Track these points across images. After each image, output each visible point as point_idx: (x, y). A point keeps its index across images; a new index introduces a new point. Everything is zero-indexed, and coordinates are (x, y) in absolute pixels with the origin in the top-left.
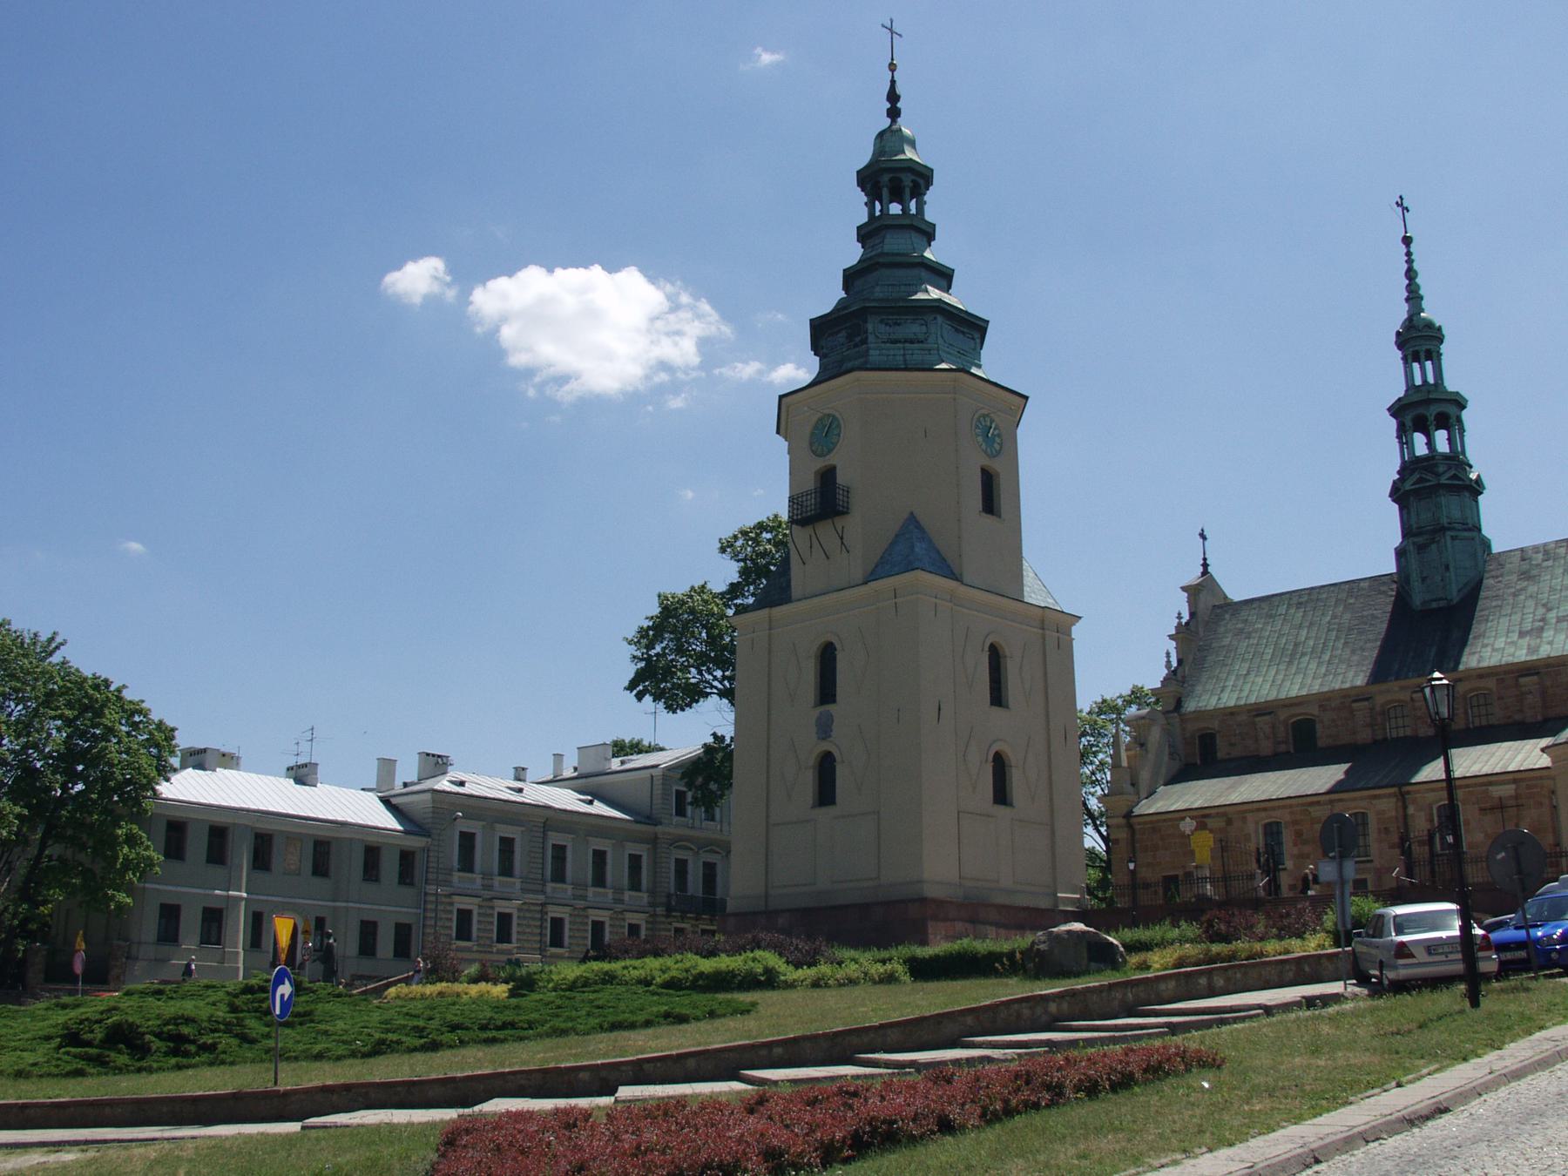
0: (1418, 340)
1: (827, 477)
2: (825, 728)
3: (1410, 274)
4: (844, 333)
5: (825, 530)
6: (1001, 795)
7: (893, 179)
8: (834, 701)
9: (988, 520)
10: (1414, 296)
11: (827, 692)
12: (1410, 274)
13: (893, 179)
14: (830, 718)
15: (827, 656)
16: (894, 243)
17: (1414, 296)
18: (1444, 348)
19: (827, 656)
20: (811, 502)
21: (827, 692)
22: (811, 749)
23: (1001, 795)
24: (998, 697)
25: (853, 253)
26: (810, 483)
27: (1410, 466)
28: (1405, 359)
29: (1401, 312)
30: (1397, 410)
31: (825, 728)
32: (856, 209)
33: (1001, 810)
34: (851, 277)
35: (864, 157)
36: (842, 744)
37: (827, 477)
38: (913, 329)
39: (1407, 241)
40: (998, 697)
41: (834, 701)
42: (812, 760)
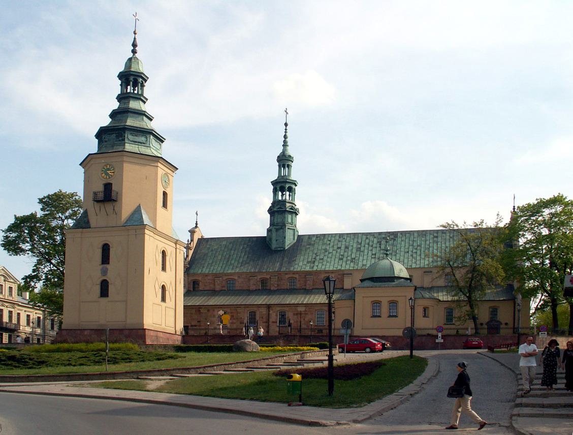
0: (284, 160)
1: (108, 187)
2: (104, 272)
3: (285, 137)
4: (115, 135)
5: (109, 206)
6: (163, 299)
7: (131, 79)
8: (108, 263)
9: (163, 210)
10: (285, 144)
11: (105, 259)
12: (285, 137)
13: (131, 79)
14: (107, 269)
15: (106, 249)
16: (133, 104)
17: (285, 144)
18: (293, 164)
19: (106, 249)
20: (101, 196)
21: (105, 259)
22: (98, 278)
23: (163, 299)
24: (164, 269)
25: (116, 105)
26: (101, 188)
27: (276, 203)
28: (279, 166)
29: (280, 150)
30: (274, 183)
31: (104, 272)
32: (116, 87)
33: (163, 304)
34: (113, 115)
35: (122, 69)
36: (110, 277)
37: (108, 187)
38: (143, 139)
39: (286, 125)
40: (164, 269)
41: (108, 263)
42: (99, 282)
